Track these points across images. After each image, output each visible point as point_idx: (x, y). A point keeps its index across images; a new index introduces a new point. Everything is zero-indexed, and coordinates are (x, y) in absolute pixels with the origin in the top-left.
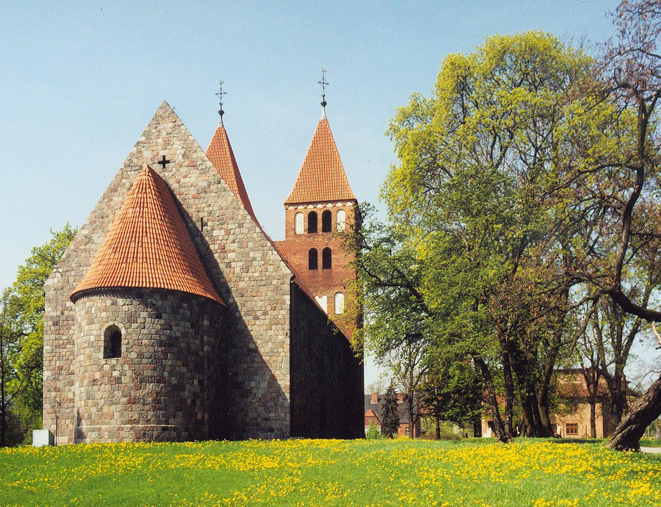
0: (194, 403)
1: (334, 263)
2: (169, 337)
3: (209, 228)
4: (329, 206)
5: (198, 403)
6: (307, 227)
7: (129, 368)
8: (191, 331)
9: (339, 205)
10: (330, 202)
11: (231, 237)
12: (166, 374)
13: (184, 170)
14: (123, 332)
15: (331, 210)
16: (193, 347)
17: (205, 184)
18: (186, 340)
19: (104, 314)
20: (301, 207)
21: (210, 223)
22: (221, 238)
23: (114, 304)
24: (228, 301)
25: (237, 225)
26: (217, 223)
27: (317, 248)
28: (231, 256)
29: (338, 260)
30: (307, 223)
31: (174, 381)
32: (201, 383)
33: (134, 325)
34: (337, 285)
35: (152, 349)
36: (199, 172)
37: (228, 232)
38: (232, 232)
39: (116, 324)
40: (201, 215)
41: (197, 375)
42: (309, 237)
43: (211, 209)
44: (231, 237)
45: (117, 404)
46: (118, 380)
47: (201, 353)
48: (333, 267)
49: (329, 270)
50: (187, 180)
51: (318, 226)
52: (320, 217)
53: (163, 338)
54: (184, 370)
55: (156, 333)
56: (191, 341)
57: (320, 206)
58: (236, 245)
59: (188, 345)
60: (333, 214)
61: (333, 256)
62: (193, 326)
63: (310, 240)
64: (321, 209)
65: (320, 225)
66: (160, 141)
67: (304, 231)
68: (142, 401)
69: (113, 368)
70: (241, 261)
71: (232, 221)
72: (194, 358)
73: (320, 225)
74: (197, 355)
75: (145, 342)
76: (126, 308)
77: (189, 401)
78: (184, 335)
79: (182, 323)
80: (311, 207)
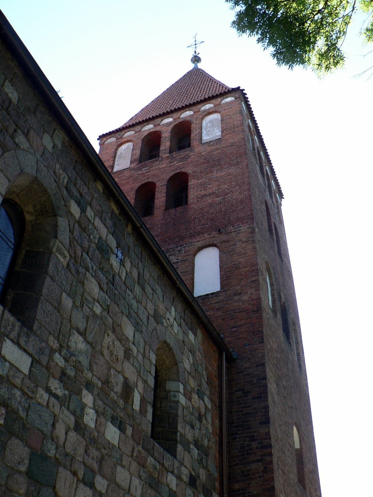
1: (193, 194)
4: (187, 114)
9: (208, 106)
20: (129, 134)
29: (204, 186)
34: (199, 233)
42: (139, 169)
48: (189, 202)
49: (179, 209)
52: (166, 135)
61: (192, 183)
64: (170, 123)
80: (149, 127)
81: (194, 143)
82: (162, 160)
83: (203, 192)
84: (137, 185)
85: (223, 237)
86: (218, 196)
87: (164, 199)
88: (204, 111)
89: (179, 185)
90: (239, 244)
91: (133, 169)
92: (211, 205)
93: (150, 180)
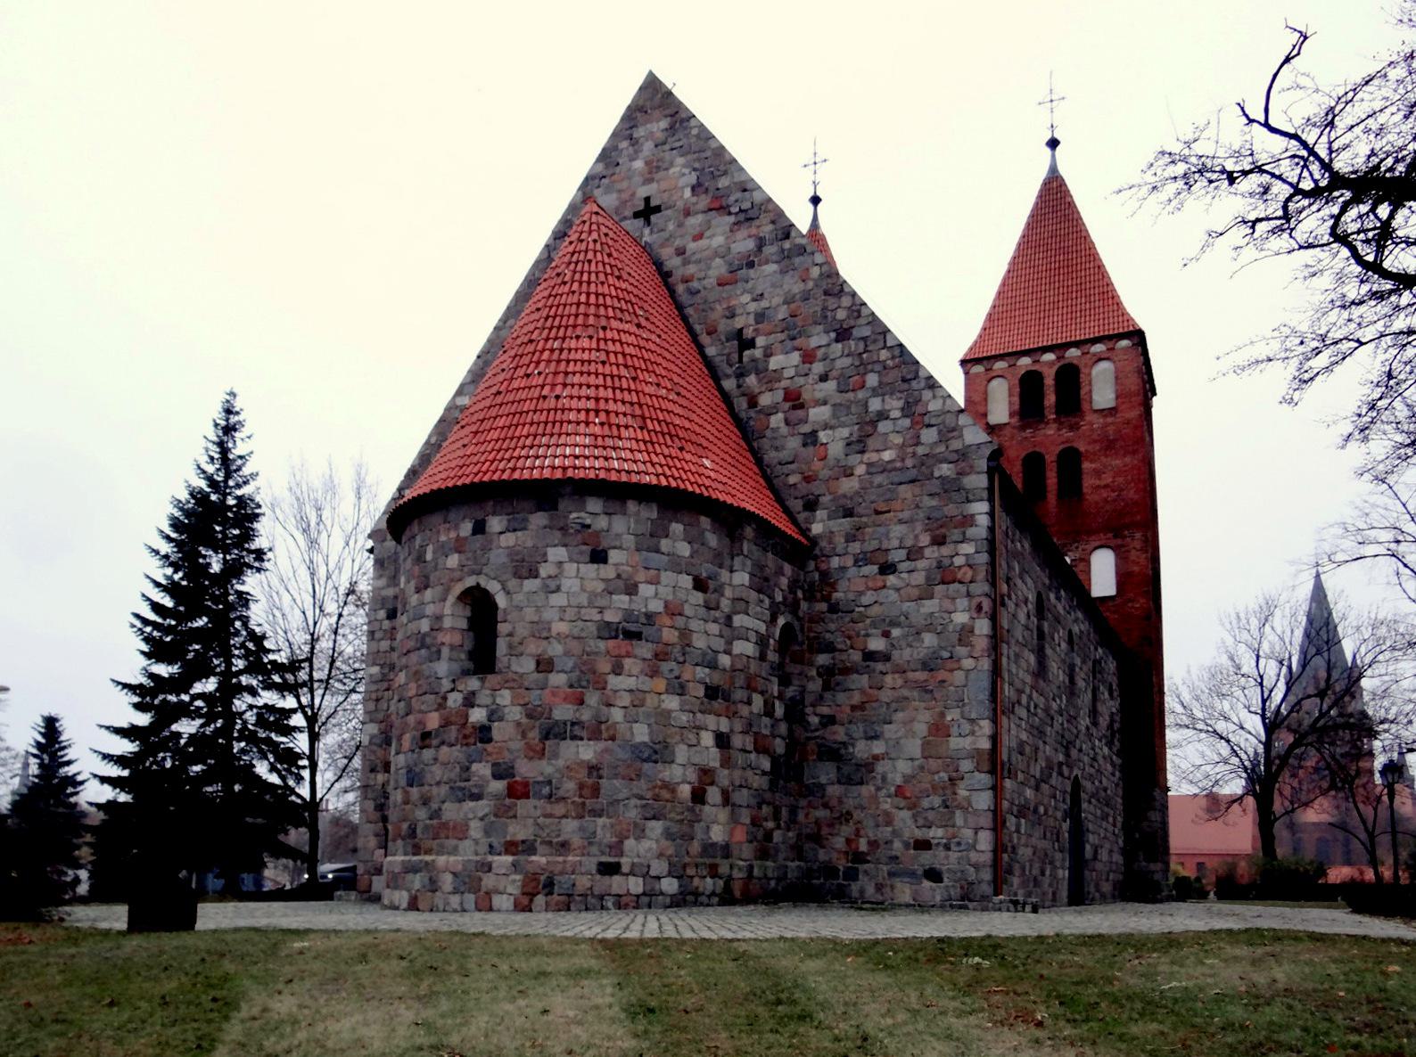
0: (699, 796)
2: (629, 615)
3: (758, 353)
4: (1073, 353)
5: (713, 794)
6: (1017, 407)
7: (513, 697)
8: (699, 597)
9: (1099, 348)
10: (1077, 344)
11: (818, 368)
12: (617, 715)
13: (695, 221)
14: (501, 601)
15: (1075, 362)
16: (699, 642)
17: (751, 244)
18: (680, 621)
19: (453, 561)
21: (760, 341)
22: (791, 372)
23: (479, 528)
24: (809, 530)
25: (833, 335)
26: (781, 336)
27: (1042, 450)
28: (818, 414)
29: (1098, 473)
30: (1016, 399)
31: (641, 734)
32: (722, 741)
33: (531, 585)
35: (575, 646)
36: (732, 219)
37: (808, 357)
38: (820, 353)
39: (483, 582)
40: (739, 323)
41: (711, 721)
42: (1023, 428)
43: (764, 304)
44: (818, 368)
45: (477, 797)
46: (484, 733)
47: (725, 660)
50: (703, 243)
51: (1047, 403)
52: (1049, 381)
53: (611, 617)
54: (672, 703)
55: (591, 605)
56: (695, 625)
57: (1049, 357)
58: (831, 385)
59: (685, 634)
60: (1084, 370)
61: (1086, 465)
62: (700, 585)
63: (1024, 434)
64: (1051, 364)
65: (1050, 399)
66: (639, 164)
67: (1011, 415)
68: (546, 790)
69: (470, 701)
70: (843, 425)
71: (820, 328)
72: (702, 672)
73: (1050, 399)
74: (713, 665)
75: (560, 627)
76: (509, 540)
77: (685, 791)
78: (673, 610)
79: (667, 577)
81: (1085, 406)
82: (1047, 423)
83: (1098, 482)
84: (1024, 454)
85: (1119, 542)
86: (1113, 491)
87: (1055, 480)
88: (1094, 355)
89: (1070, 460)
90: (1133, 552)
91: (1014, 428)
92: (1106, 501)
93: (1037, 449)
